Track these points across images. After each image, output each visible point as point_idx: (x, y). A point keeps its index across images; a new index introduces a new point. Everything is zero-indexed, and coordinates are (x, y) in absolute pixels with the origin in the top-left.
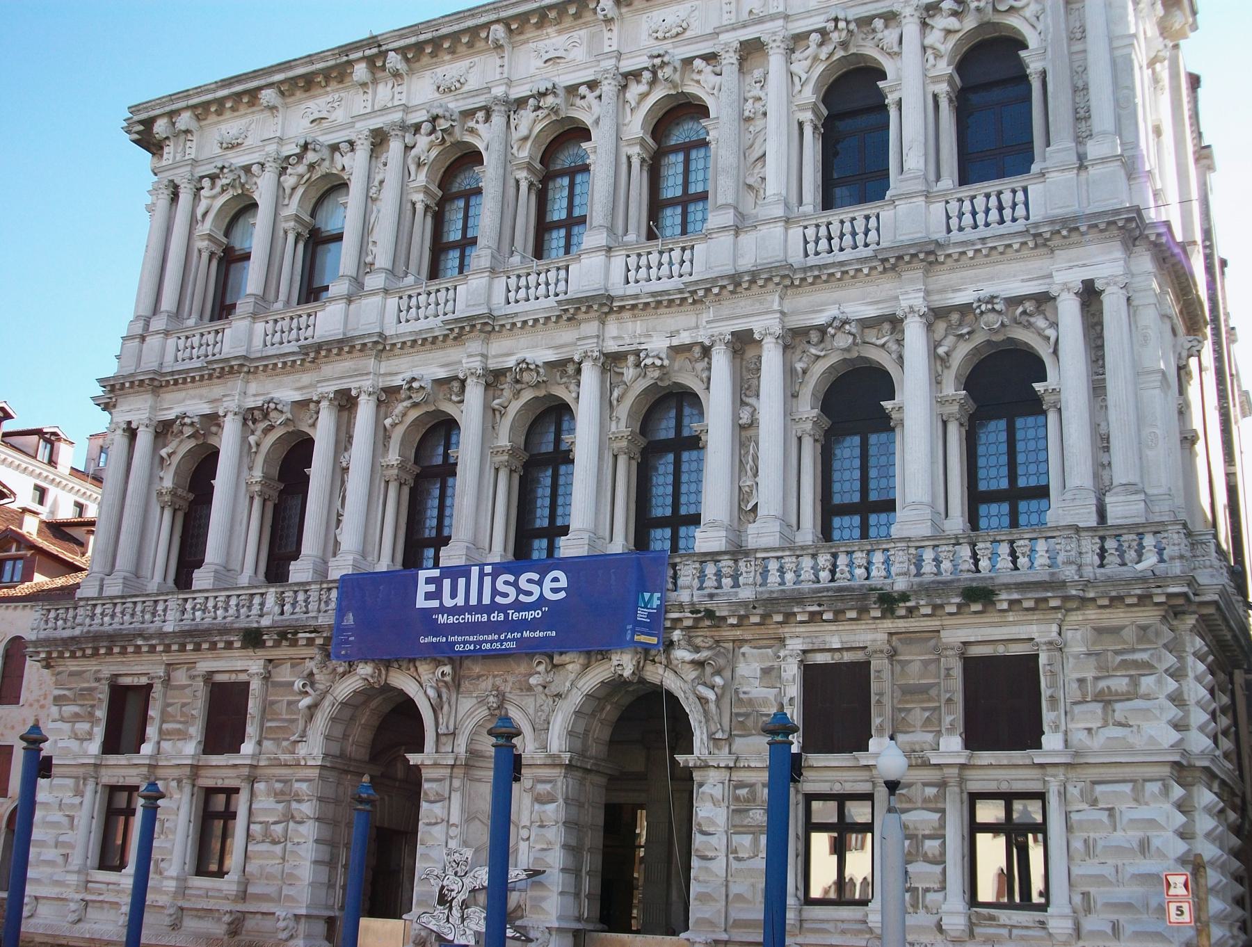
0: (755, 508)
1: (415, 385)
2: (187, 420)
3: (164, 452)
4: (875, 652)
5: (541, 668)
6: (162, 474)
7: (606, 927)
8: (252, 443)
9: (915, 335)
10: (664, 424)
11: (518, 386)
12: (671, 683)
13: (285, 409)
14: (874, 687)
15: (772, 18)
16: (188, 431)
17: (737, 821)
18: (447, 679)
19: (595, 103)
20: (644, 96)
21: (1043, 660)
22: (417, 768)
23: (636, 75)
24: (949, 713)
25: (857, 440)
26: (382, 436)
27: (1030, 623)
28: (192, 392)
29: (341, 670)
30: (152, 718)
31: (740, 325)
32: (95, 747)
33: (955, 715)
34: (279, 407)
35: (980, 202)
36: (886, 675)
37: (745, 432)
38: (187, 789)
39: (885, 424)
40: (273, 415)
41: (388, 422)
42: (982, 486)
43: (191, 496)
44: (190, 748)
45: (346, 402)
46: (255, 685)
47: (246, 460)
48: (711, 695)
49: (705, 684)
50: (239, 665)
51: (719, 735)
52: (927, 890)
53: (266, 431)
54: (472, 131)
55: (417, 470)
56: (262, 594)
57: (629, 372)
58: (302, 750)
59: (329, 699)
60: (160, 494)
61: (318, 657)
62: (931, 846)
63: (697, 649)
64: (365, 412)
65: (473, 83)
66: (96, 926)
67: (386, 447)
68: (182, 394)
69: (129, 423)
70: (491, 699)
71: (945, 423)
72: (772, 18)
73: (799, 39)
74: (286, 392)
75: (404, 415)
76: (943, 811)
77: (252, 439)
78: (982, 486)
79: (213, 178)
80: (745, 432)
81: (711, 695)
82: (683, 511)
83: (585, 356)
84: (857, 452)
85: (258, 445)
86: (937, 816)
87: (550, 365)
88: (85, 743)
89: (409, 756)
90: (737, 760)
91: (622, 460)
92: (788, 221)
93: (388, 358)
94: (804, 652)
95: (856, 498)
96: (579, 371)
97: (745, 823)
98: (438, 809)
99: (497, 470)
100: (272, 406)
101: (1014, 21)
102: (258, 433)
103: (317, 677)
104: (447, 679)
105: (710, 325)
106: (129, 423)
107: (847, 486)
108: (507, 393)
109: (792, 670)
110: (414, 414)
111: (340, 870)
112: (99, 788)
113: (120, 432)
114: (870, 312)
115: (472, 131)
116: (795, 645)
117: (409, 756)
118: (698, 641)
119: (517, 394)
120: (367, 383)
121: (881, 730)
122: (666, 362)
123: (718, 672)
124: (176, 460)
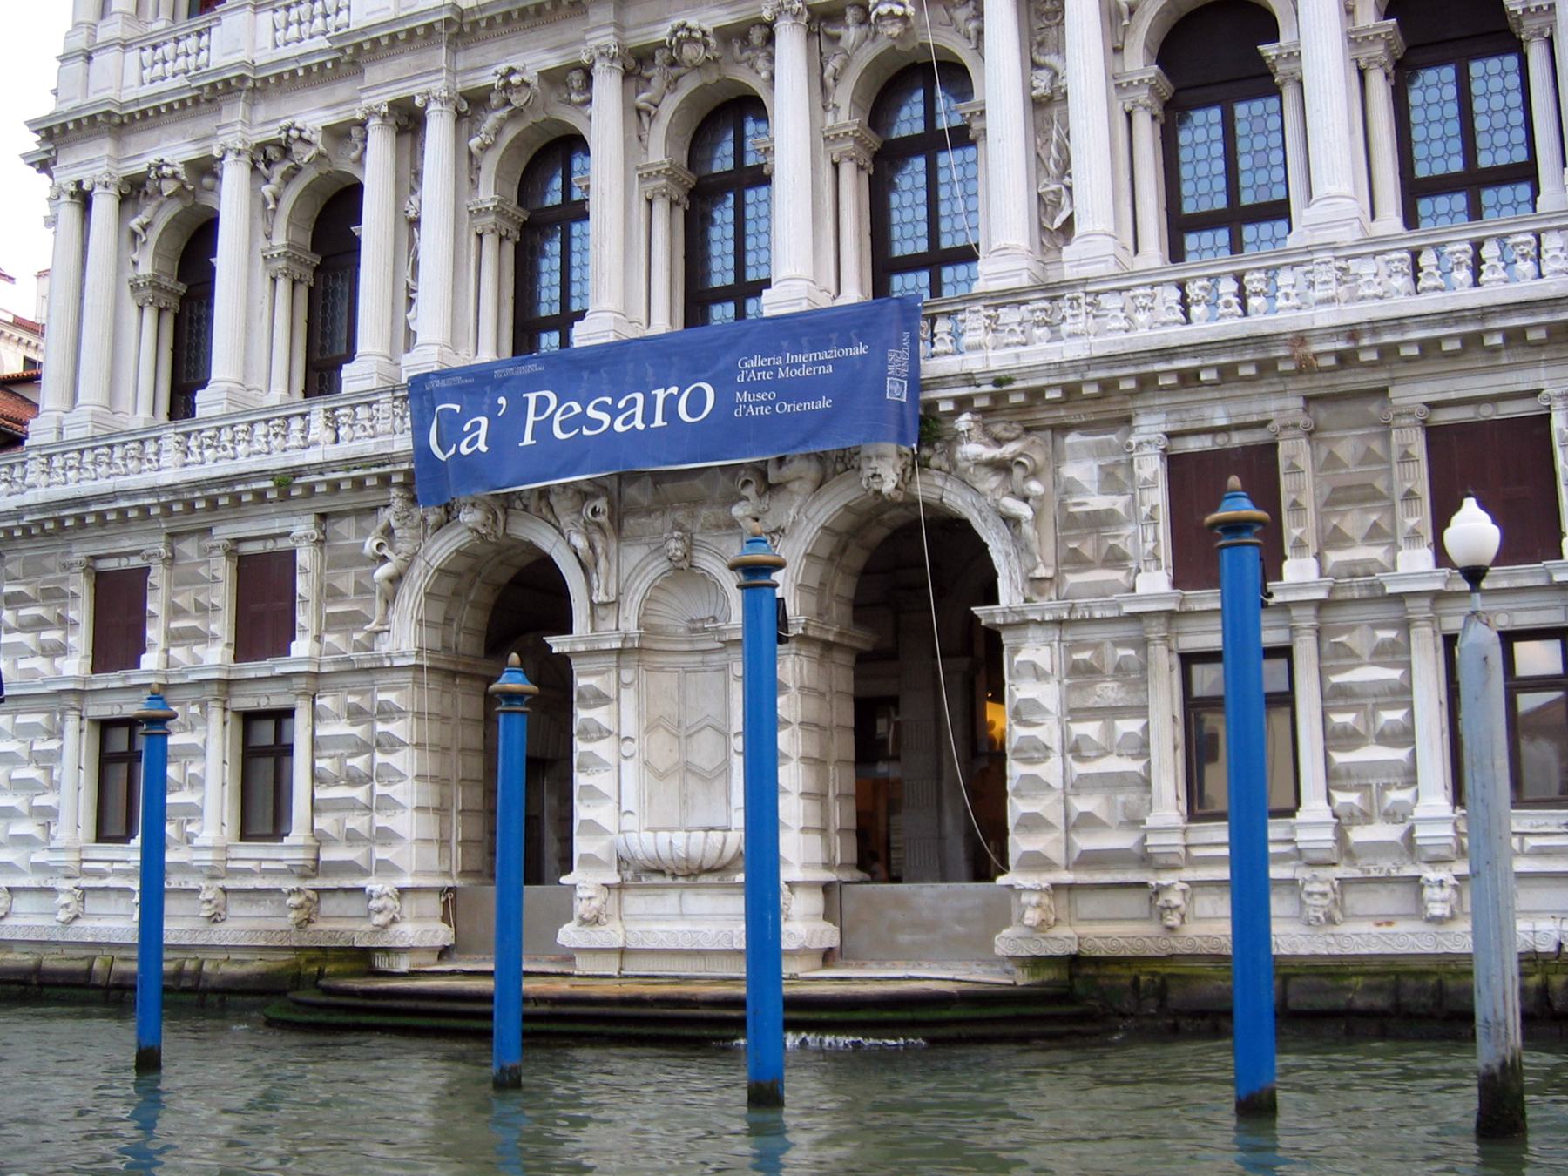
1: (515, 79)
2: (165, 170)
3: (135, 223)
4: (1285, 427)
5: (750, 491)
6: (135, 257)
7: (867, 877)
8: (269, 195)
10: (905, 113)
11: (675, 71)
13: (314, 138)
14: (1285, 482)
16: (169, 187)
17: (1076, 702)
18: (603, 519)
22: (565, 659)
24: (1410, 514)
25: (1215, 114)
26: (468, 164)
27: (1535, 364)
28: (171, 129)
29: (431, 519)
30: (154, 616)
32: (75, 666)
34: (305, 135)
36: (1304, 462)
37: (1045, 107)
38: (216, 716)
39: (1262, 82)
40: (296, 147)
41: (475, 143)
42: (1421, 171)
43: (182, 288)
44: (216, 655)
45: (408, 121)
46: (304, 557)
47: (260, 224)
48: (1024, 511)
49: (1013, 494)
50: (277, 526)
51: (1041, 572)
52: (1387, 787)
53: (288, 177)
55: (523, 216)
56: (303, 415)
58: (384, 646)
59: (420, 563)
60: (135, 287)
61: (397, 504)
63: (999, 442)
64: (438, 131)
66: (97, 924)
67: (474, 183)
68: (156, 133)
69: (79, 184)
70: (672, 544)
71: (1362, 74)
74: (311, 115)
75: (498, 132)
76: (1408, 666)
77: (267, 190)
78: (1421, 171)
80: (1045, 107)
81: (1024, 511)
82: (946, 243)
83: (780, 11)
84: (1217, 132)
85: (277, 200)
86: (1395, 674)
87: (721, 32)
88: (58, 661)
89: (550, 640)
90: (1072, 609)
91: (847, 170)
93: (466, 47)
94: (1170, 435)
95: (1220, 202)
96: (770, 39)
97: (1090, 703)
98: (601, 715)
99: (650, 202)
100: (294, 133)
102: (276, 179)
103: (398, 533)
104: (603, 519)
106: (79, 184)
107: (1203, 186)
108: (657, 84)
109: (1152, 467)
110: (510, 133)
111: (456, 818)
112: (85, 723)
113: (65, 198)
116: (1151, 427)
117: (550, 640)
118: (998, 429)
119: (673, 84)
120: (438, 86)
121: (1300, 545)
122: (911, 10)
123: (1034, 474)
124: (153, 236)
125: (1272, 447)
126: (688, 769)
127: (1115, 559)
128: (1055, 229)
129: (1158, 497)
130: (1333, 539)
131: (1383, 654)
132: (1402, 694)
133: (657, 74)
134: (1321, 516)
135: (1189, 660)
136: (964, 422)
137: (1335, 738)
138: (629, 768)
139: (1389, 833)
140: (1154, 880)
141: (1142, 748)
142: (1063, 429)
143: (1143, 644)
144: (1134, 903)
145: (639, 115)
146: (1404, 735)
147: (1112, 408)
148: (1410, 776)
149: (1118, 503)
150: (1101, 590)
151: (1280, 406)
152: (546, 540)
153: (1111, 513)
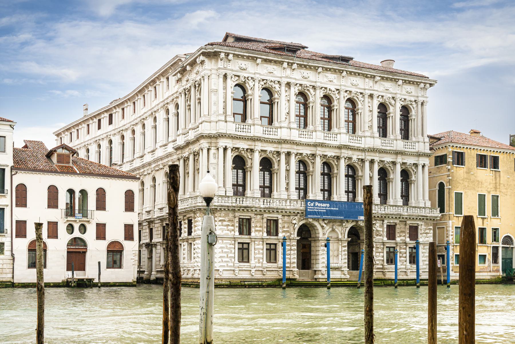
15: (376, 91)
19: (337, 95)
21: (420, 227)
31: (373, 158)
54: (308, 90)
62: (405, 255)
72: (376, 91)
79: (235, 75)
83: (343, 157)
105: (369, 157)
109: (385, 226)
115: (308, 90)
116: (386, 222)
129: (385, 230)
131: (404, 249)
132: (406, 253)
137: (400, 257)
139: (404, 267)
144: (381, 273)
146: (406, 257)
147: (382, 219)
148: (406, 261)
149: (381, 229)
150: (379, 239)
151: (397, 221)
152: (316, 223)
153: (380, 231)
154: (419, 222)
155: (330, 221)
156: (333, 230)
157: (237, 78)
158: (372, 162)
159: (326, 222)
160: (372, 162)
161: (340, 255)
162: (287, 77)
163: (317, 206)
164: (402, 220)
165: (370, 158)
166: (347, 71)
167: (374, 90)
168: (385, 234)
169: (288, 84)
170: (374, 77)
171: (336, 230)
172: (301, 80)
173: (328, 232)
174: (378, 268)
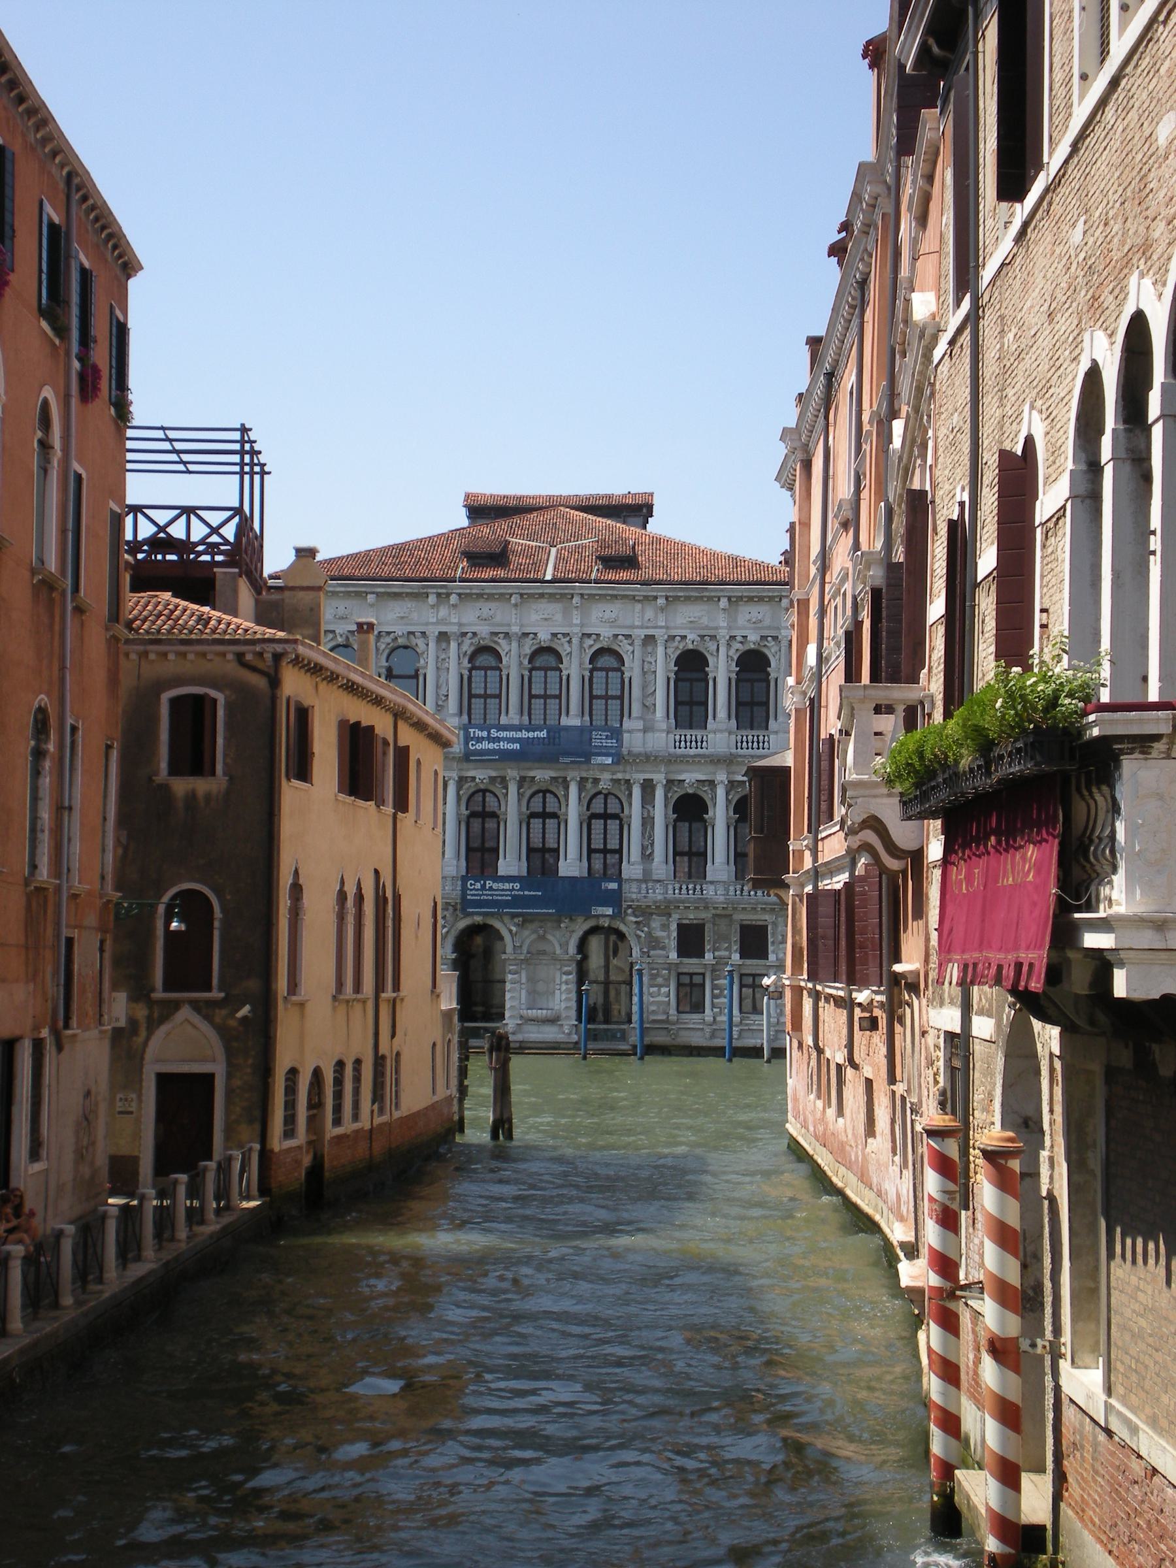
0: (652, 854)
9: (721, 792)
12: (623, 928)
15: (661, 627)
19: (566, 646)
20: (591, 646)
23: (589, 636)
31: (648, 776)
33: (736, 947)
35: (750, 738)
57: (589, 785)
63: (636, 916)
65: (498, 618)
72: (661, 627)
73: (672, 638)
92: (668, 733)
101: (765, 651)
109: (674, 927)
114: (703, 778)
125: (704, 925)
126: (535, 992)
127: (663, 948)
128: (647, 856)
129: (675, 934)
130: (714, 950)
133: (526, 785)
134: (715, 943)
135: (679, 974)
136: (630, 911)
137: (714, 996)
138: (524, 992)
140: (670, 1027)
141: (669, 996)
142: (652, 914)
143: (669, 970)
144: (664, 1032)
145: (520, 796)
149: (664, 934)
150: (659, 956)
152: (497, 924)
153: (663, 937)
154: (767, 917)
155: (526, 920)
156: (542, 938)
157: (331, 636)
158: (648, 787)
159: (516, 920)
160: (648, 787)
161: (557, 992)
162: (438, 623)
163: (491, 889)
164: (718, 912)
165: (642, 777)
166: (582, 595)
167: (656, 627)
168: (673, 944)
169: (443, 637)
170: (656, 598)
171: (549, 937)
172: (475, 625)
173: (528, 942)
174: (654, 1021)
